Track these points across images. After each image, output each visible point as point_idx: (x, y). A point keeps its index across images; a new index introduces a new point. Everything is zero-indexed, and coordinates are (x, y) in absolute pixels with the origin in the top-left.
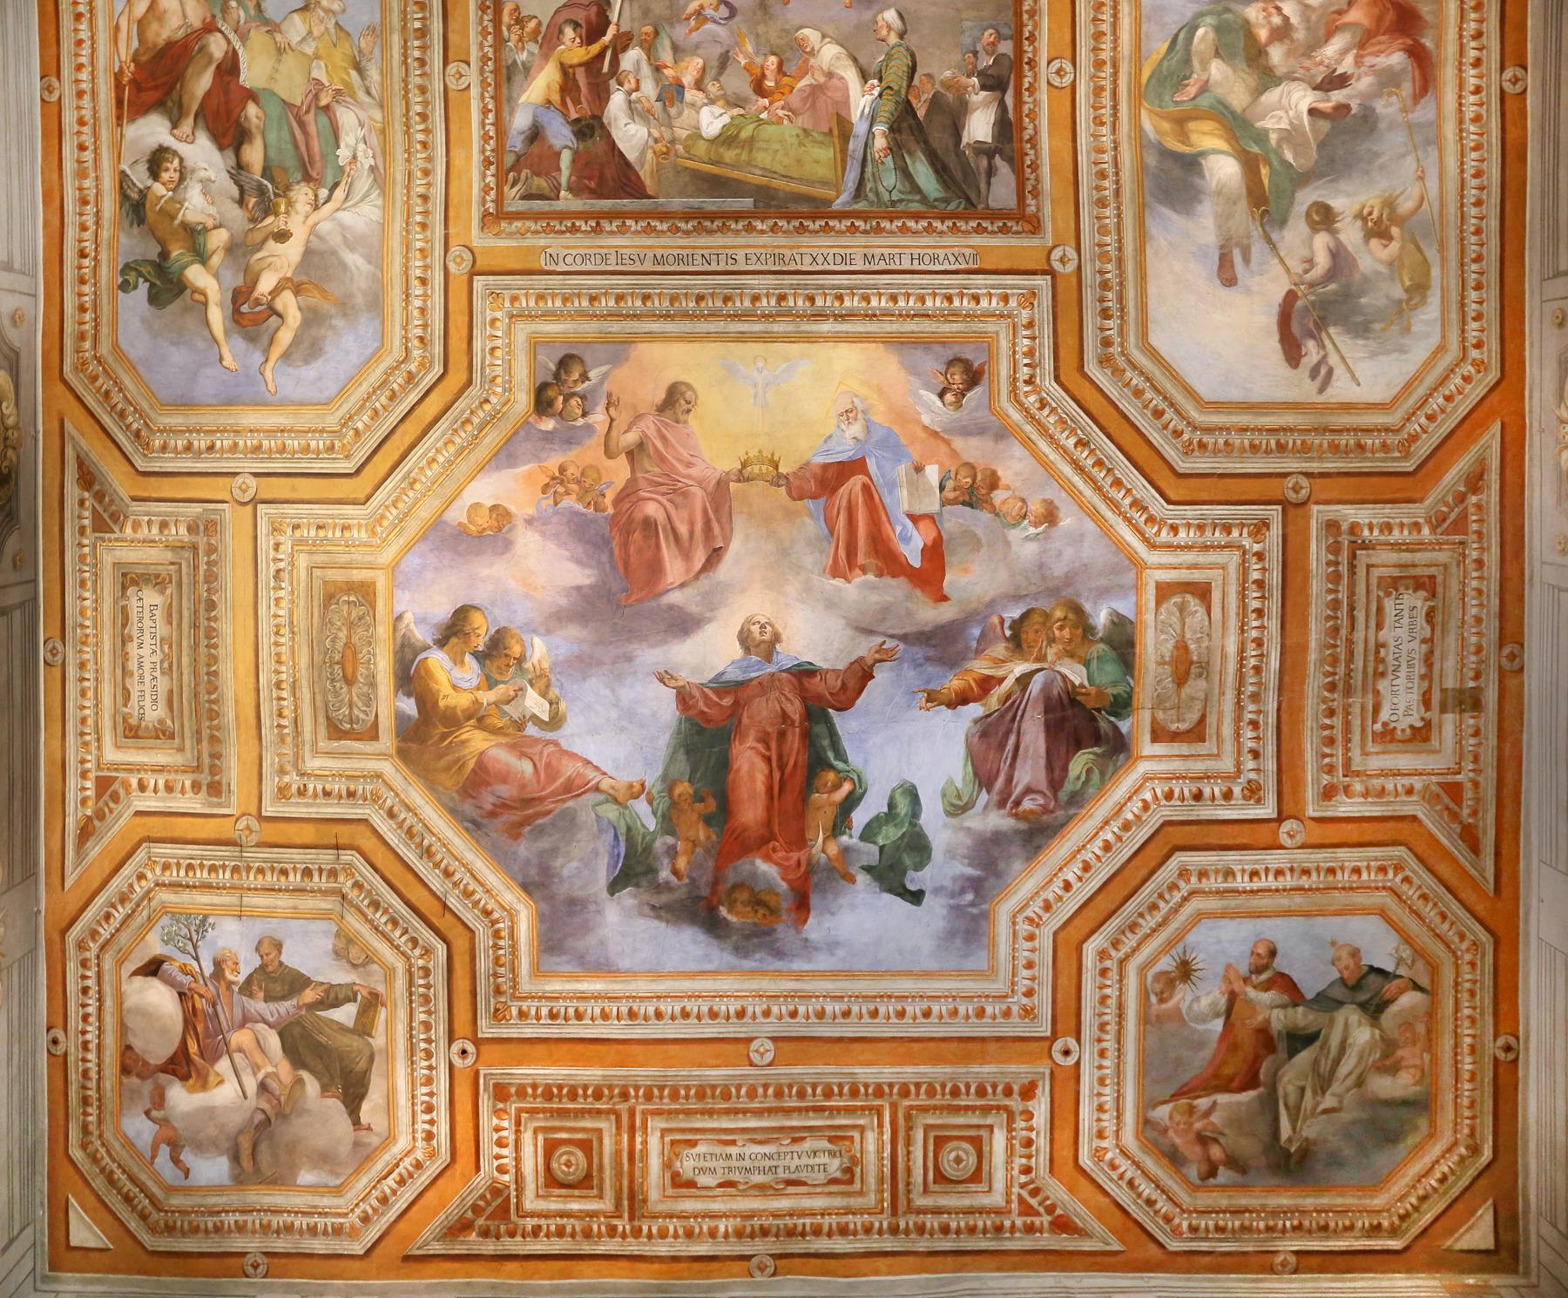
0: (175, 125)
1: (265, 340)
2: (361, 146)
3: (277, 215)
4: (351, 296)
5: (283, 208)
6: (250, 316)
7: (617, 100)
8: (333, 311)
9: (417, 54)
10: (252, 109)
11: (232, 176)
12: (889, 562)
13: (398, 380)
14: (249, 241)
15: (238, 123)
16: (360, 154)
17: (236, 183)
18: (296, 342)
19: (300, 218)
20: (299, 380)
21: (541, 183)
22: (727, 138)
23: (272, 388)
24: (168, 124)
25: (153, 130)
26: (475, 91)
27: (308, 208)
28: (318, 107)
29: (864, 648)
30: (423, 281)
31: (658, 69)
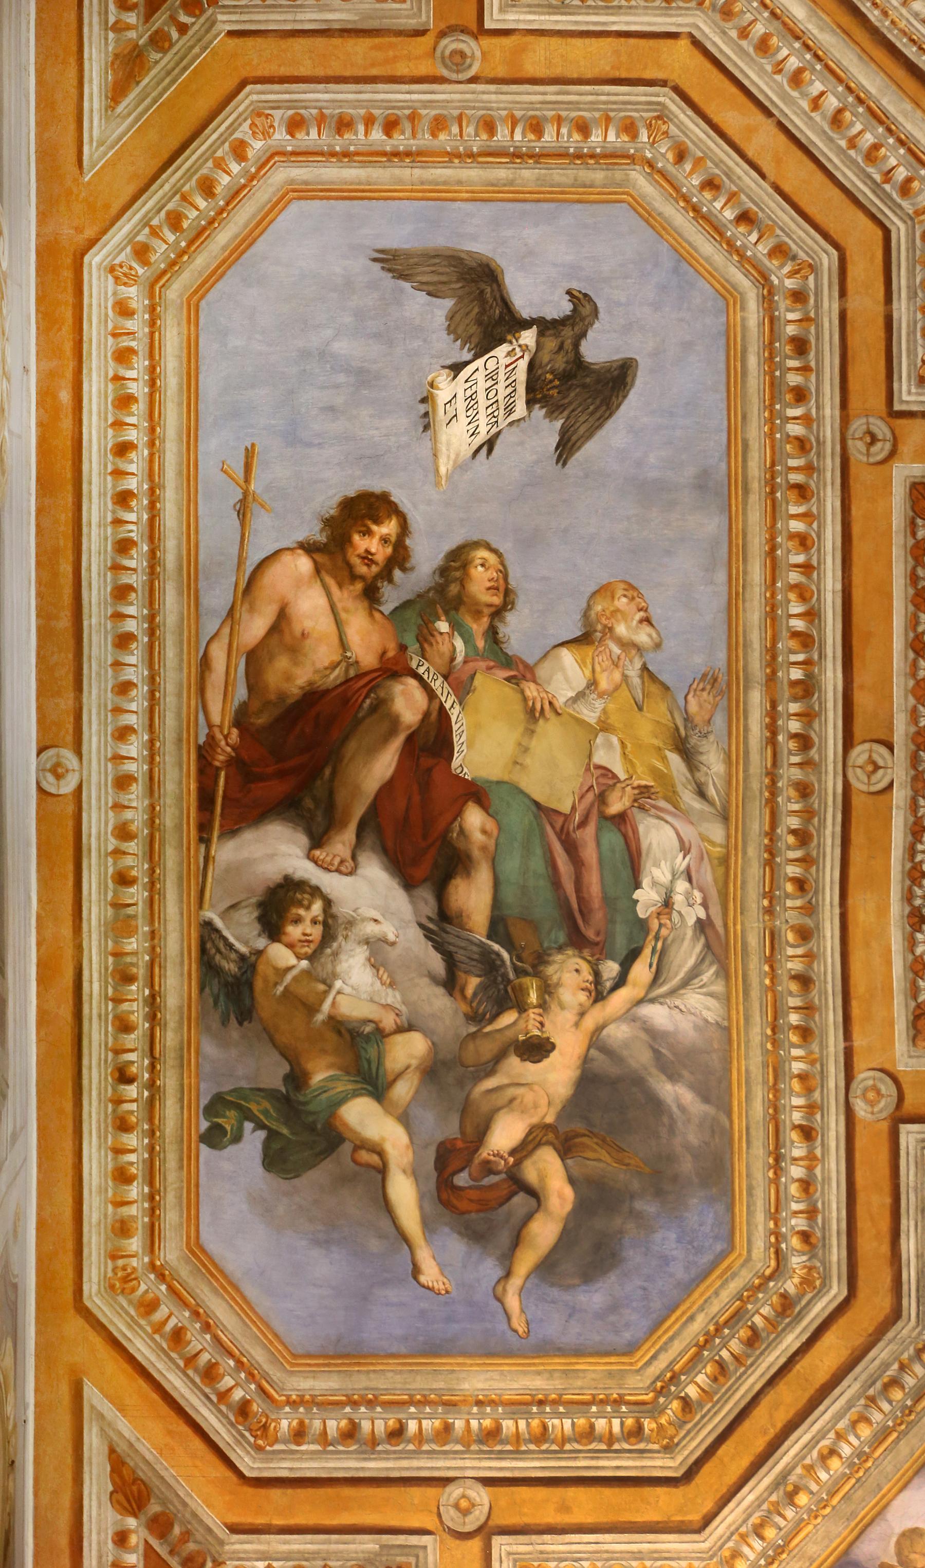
0: (317, 840)
1: (504, 1238)
2: (682, 886)
3: (522, 1008)
4: (671, 1158)
5: (533, 997)
8: (636, 1185)
9: (795, 726)
10: (474, 818)
11: (429, 934)
13: (762, 1313)
14: (470, 1055)
15: (444, 836)
16: (678, 899)
17: (439, 947)
19: (569, 1016)
20: (573, 1312)
23: (519, 1324)
24: (303, 840)
25: (278, 851)
26: (900, 796)
27: (582, 997)
28: (604, 817)
30: (807, 1133)
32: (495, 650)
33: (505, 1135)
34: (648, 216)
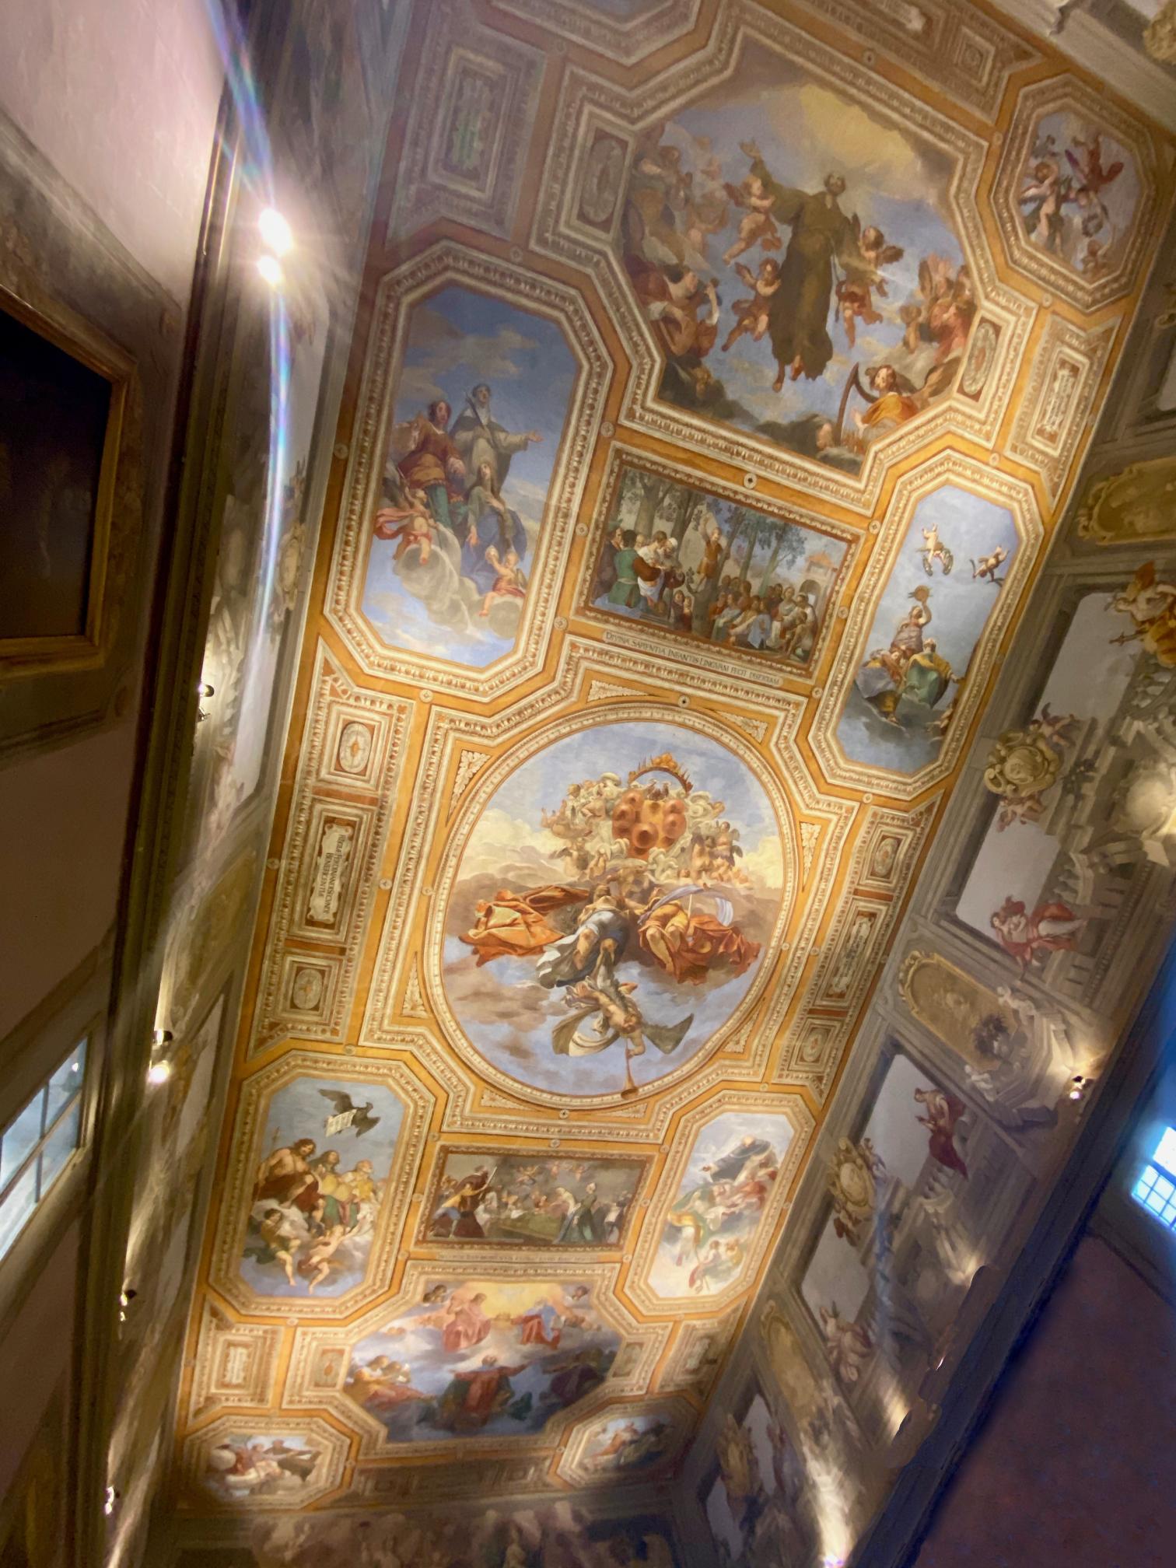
6: (305, 1269)
7: (481, 1207)
12: (540, 1339)
18: (325, 1279)
21: (442, 1230)
22: (520, 1219)
29: (525, 1362)
31: (499, 1199)
32: (333, 1171)
33: (315, 1260)
34: (390, 1087)
